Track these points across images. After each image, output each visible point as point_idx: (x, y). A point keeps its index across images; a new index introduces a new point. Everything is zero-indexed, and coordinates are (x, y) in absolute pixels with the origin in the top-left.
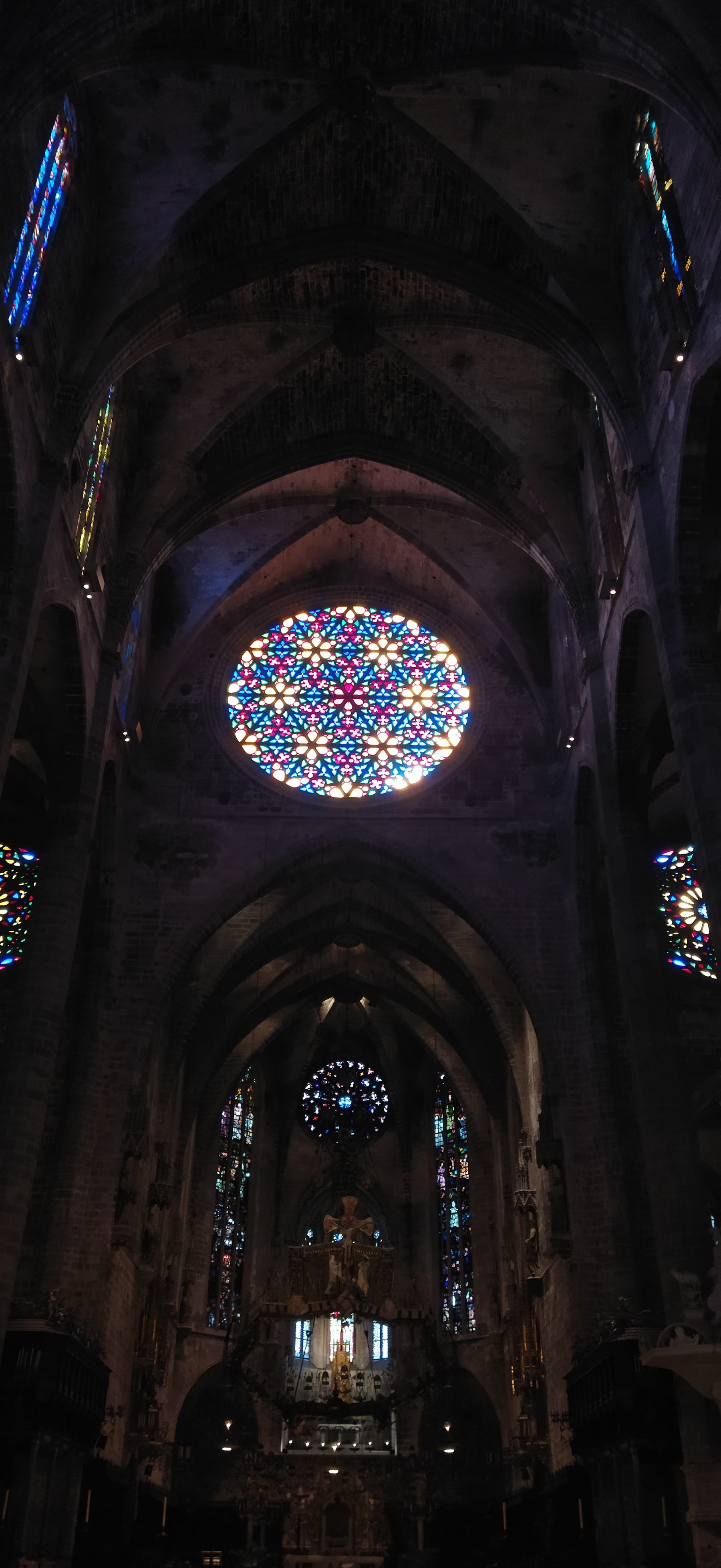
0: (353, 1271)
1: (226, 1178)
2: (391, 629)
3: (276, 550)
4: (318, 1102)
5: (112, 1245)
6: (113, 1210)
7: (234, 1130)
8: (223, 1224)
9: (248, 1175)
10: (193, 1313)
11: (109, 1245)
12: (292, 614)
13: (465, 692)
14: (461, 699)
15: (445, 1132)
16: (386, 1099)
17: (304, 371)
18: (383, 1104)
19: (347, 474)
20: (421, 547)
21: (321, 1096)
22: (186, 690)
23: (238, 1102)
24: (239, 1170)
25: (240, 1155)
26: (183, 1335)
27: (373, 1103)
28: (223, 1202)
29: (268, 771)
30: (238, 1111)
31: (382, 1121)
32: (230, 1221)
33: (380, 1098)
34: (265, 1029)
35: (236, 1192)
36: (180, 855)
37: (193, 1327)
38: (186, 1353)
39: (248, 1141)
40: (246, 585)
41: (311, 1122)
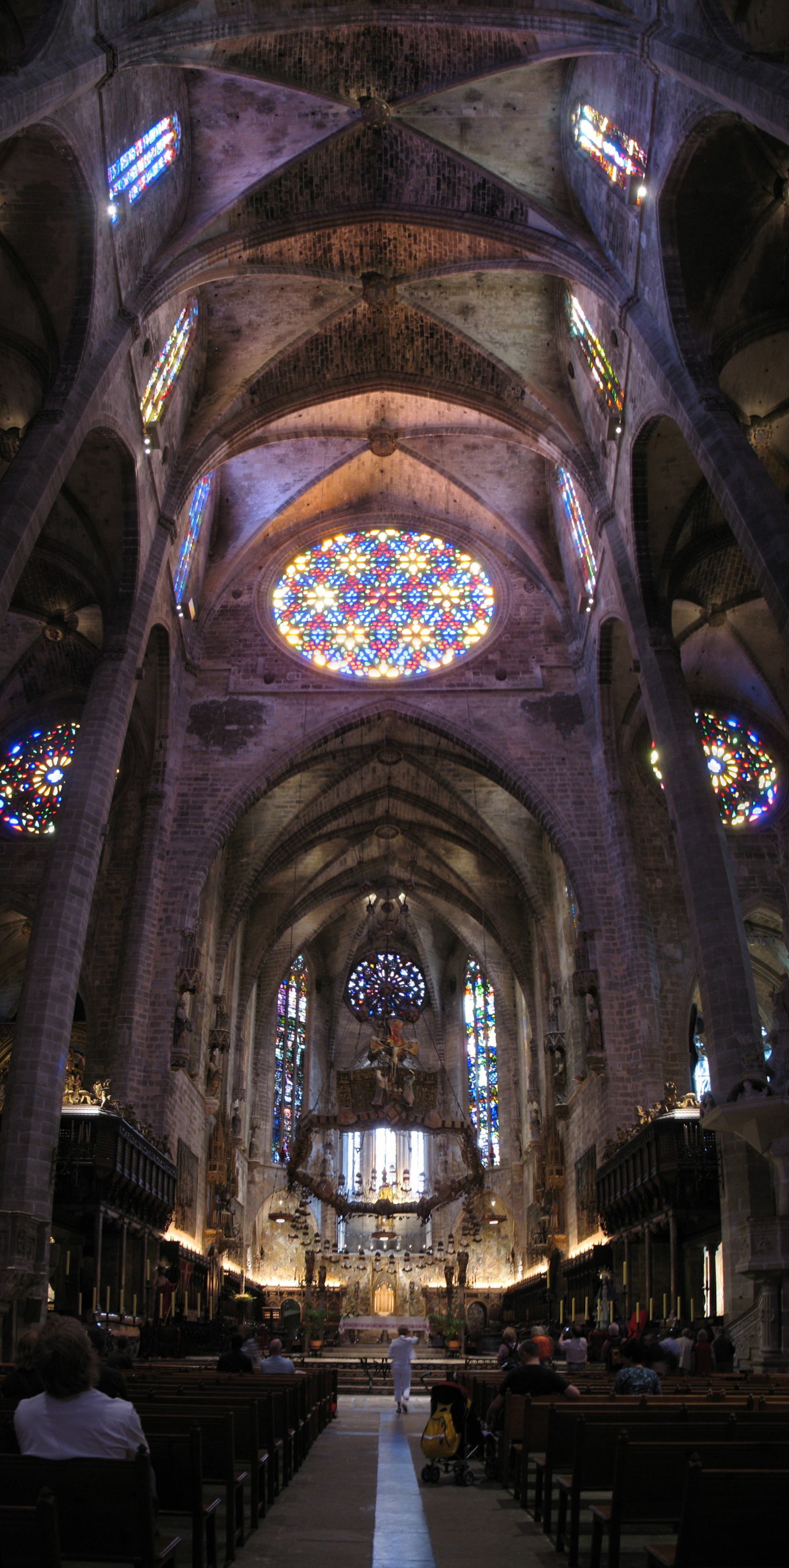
1: (284, 1048)
2: (419, 546)
3: (318, 479)
4: (364, 990)
5: (173, 1065)
6: (171, 1035)
8: (283, 1084)
9: (303, 1047)
10: (261, 1151)
11: (169, 1066)
12: (332, 536)
13: (489, 591)
14: (485, 597)
15: (475, 1010)
16: (422, 985)
17: (340, 324)
18: (420, 990)
19: (377, 412)
20: (442, 472)
21: (367, 983)
22: (237, 594)
23: (292, 987)
24: (294, 1043)
25: (295, 1031)
27: (411, 989)
28: (282, 1067)
29: (310, 657)
30: (293, 994)
31: (419, 1002)
32: (289, 1082)
33: (417, 985)
35: (293, 1059)
37: (261, 1161)
38: (257, 1179)
39: (302, 1019)
40: (290, 511)
41: (357, 1004)
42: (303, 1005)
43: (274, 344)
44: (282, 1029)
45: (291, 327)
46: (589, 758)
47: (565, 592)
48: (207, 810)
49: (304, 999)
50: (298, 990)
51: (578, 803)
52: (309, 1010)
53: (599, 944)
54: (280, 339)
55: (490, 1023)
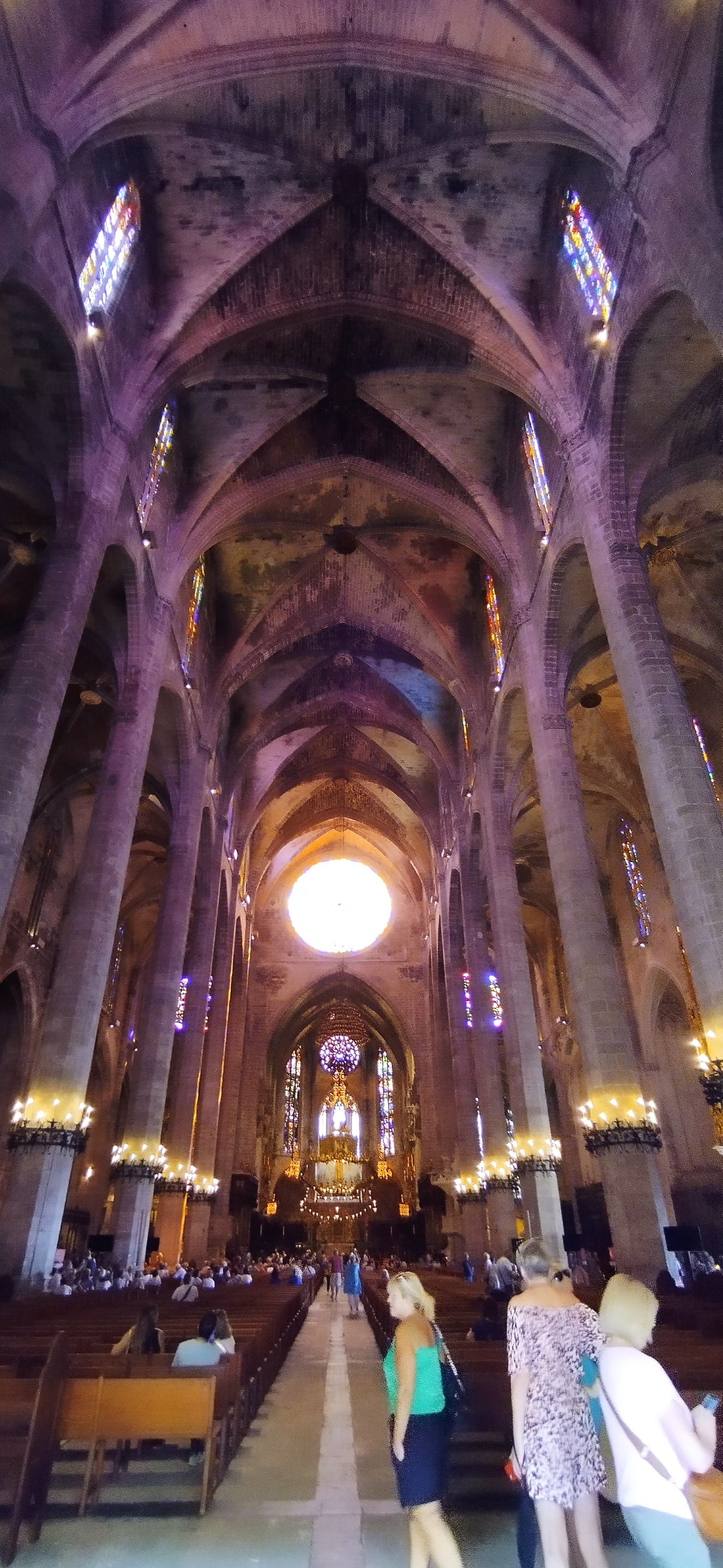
0: (344, 1147)
1: (290, 1090)
6: (256, 1124)
7: (292, 1069)
8: (289, 1110)
20: (369, 840)
22: (273, 903)
24: (295, 1087)
26: (274, 1157)
32: (292, 1108)
34: (306, 1029)
35: (294, 1096)
36: (274, 979)
42: (299, 1066)
43: (290, 802)
44: (289, 1080)
45: (297, 793)
46: (423, 997)
47: (421, 907)
48: (267, 1021)
49: (299, 1062)
50: (296, 1058)
51: (417, 1019)
52: (301, 1069)
53: (421, 1083)
54: (292, 800)
55: (389, 1077)
